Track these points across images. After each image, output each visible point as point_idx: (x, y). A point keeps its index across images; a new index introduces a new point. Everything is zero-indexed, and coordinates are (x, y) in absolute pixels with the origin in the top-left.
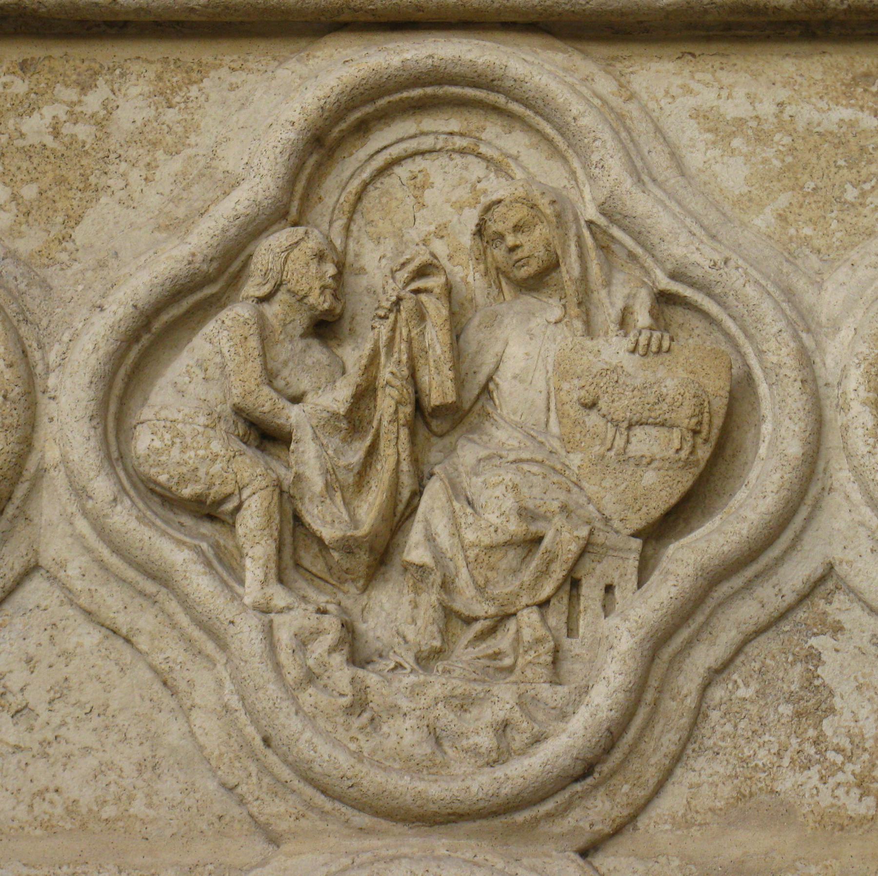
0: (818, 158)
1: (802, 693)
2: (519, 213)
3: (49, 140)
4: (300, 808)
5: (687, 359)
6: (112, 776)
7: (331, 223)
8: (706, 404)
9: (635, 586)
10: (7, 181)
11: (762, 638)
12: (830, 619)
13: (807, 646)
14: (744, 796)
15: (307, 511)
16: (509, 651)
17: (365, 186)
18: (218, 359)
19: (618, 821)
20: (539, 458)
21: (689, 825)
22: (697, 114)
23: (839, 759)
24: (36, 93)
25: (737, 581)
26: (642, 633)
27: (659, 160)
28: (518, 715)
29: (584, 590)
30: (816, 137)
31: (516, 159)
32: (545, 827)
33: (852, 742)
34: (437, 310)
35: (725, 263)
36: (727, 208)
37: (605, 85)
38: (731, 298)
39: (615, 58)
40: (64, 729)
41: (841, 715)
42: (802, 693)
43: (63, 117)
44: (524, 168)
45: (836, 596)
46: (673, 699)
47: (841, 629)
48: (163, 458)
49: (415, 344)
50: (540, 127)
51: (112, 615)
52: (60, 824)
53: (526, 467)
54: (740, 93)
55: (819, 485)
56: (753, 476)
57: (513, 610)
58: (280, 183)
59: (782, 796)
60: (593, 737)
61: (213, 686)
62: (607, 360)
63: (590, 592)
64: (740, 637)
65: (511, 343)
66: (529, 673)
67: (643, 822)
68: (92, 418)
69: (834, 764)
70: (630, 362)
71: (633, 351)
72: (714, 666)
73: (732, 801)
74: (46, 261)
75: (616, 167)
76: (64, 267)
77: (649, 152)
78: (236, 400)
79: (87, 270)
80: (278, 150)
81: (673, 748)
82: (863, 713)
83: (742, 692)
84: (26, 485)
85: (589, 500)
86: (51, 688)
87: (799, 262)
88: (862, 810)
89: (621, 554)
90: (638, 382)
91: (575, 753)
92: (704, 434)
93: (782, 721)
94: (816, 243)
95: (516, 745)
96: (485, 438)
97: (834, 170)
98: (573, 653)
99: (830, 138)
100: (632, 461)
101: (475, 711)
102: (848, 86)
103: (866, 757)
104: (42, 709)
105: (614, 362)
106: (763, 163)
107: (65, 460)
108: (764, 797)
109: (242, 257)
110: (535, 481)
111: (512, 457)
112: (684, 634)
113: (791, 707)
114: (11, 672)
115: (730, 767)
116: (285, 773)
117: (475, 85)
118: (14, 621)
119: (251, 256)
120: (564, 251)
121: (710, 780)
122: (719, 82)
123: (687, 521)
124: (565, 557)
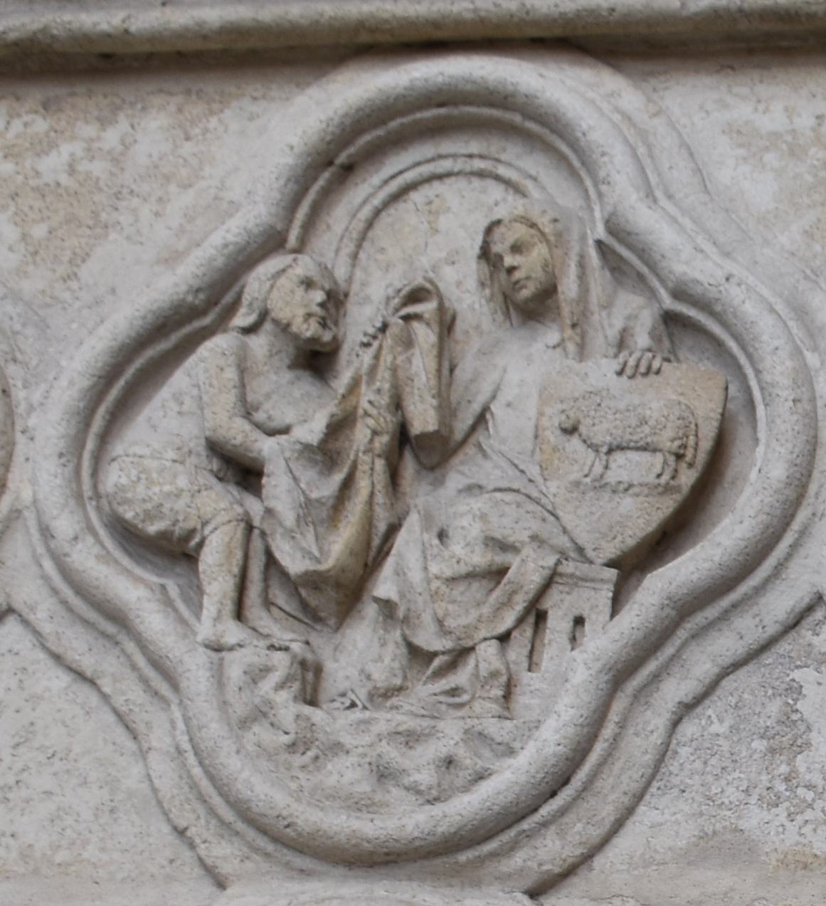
2: (520, 231)
4: (245, 849)
6: (69, 821)
7: (337, 251)
8: (693, 426)
9: (608, 618)
11: (742, 673)
13: (788, 679)
14: (707, 834)
15: (278, 547)
17: (377, 212)
18: (195, 392)
19: (570, 861)
23: (810, 795)
24: (56, 131)
25: (711, 612)
26: (598, 665)
27: (680, 175)
29: (551, 622)
31: (535, 179)
34: (425, 335)
40: (25, 774)
41: (817, 750)
46: (636, 734)
48: (129, 495)
49: (401, 374)
51: (77, 657)
52: (15, 868)
57: (470, 644)
58: (273, 210)
59: (746, 833)
60: (537, 772)
61: (168, 726)
63: (558, 624)
64: (716, 670)
67: (598, 861)
68: (61, 455)
69: (804, 801)
71: (620, 373)
72: (688, 700)
74: (48, 300)
76: (66, 305)
78: (208, 433)
80: (273, 176)
83: (716, 728)
90: (622, 406)
92: (689, 458)
93: (754, 757)
98: (532, 688)
100: (608, 489)
101: (420, 749)
107: (35, 502)
108: (728, 836)
109: (236, 289)
112: (651, 666)
113: (765, 742)
115: (695, 805)
116: (228, 815)
119: (243, 287)
121: (673, 819)
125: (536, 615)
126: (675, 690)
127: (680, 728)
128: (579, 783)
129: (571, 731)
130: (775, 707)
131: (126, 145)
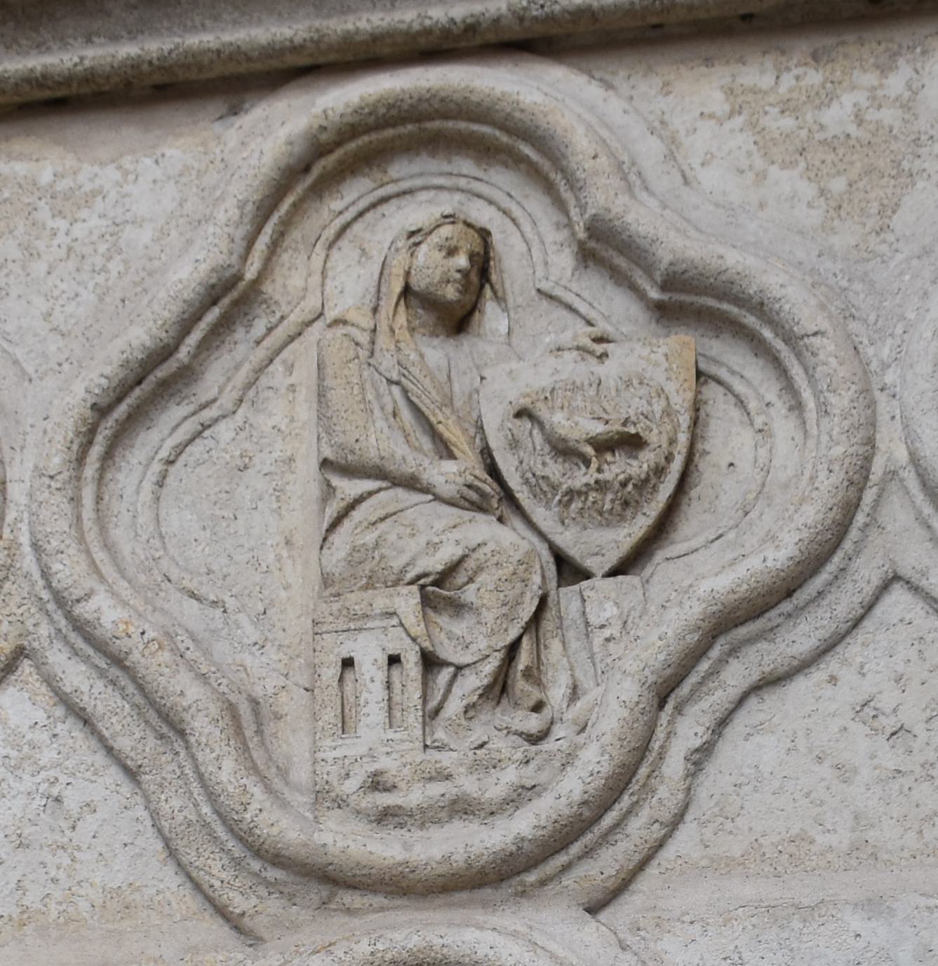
3: (852, 129)
10: (813, 176)
24: (832, 82)
43: (864, 103)
74: (865, 255)
79: (912, 258)
84: (875, 490)
86: (926, 707)
104: (919, 729)
114: (880, 692)
118: (877, 638)
131: (914, 91)
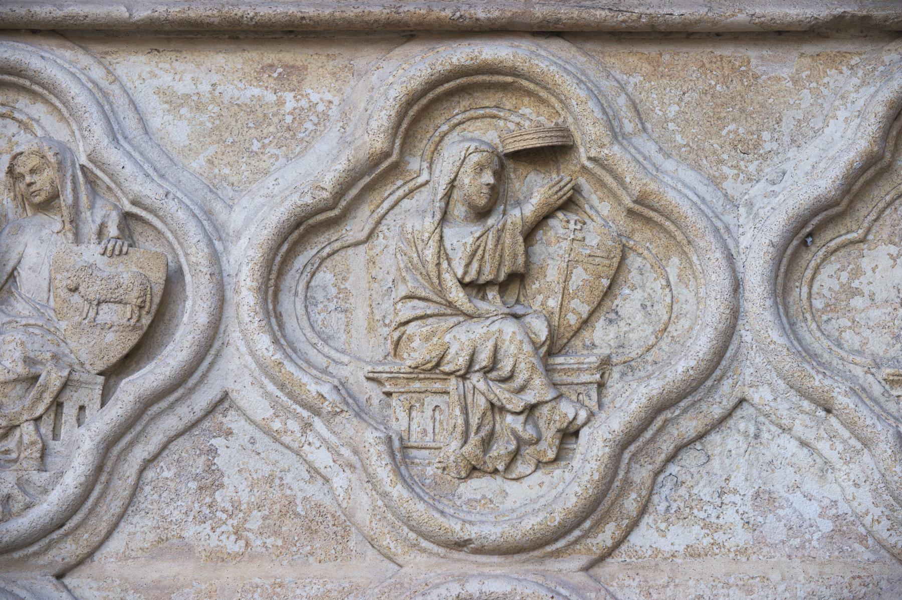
0: (236, 121)
1: (203, 474)
2: (34, 161)
5: (138, 259)
8: (149, 289)
9: (99, 407)
11: (181, 440)
12: (225, 427)
13: (209, 444)
14: (163, 540)
16: (15, 449)
19: (80, 556)
20: (40, 323)
21: (127, 558)
22: (160, 91)
23: (224, 516)
25: (164, 404)
26: (98, 438)
27: (131, 124)
28: (16, 491)
29: (66, 410)
30: (236, 107)
32: (33, 561)
33: (233, 506)
35: (166, 196)
36: (174, 155)
37: (97, 73)
38: (169, 218)
39: (107, 53)
41: (228, 488)
42: (203, 474)
44: (43, 128)
45: (230, 412)
46: (120, 479)
47: (231, 433)
50: (53, 102)
53: (31, 330)
54: (188, 77)
55: (220, 343)
56: (178, 335)
57: (18, 423)
59: (186, 540)
62: (87, 259)
63: (69, 411)
64: (165, 439)
65: (28, 245)
66: (24, 464)
67: (97, 556)
69: (221, 520)
70: (102, 261)
71: (103, 254)
72: (148, 457)
73: (154, 543)
75: (98, 130)
77: (124, 118)
81: (118, 510)
82: (241, 488)
83: (166, 474)
85: (71, 352)
87: (219, 192)
88: (237, 549)
89: (90, 386)
90: (105, 275)
91: (51, 515)
92: (147, 309)
93: (190, 492)
94: (232, 179)
95: (14, 510)
96: (10, 308)
97: (246, 129)
98: (56, 451)
99: (244, 108)
102: (258, 73)
103: (241, 515)
105: (91, 261)
106: (200, 124)
108: (175, 541)
110: (36, 339)
111: (24, 322)
112: (128, 438)
113: (196, 483)
115: (155, 522)
117: (10, 74)
120: (61, 188)
122: (175, 69)
123: (137, 363)
124: (51, 390)
125: (57, 405)
126: (140, 453)
127: (144, 474)
128: (87, 510)
129: (83, 479)
130: (201, 461)
